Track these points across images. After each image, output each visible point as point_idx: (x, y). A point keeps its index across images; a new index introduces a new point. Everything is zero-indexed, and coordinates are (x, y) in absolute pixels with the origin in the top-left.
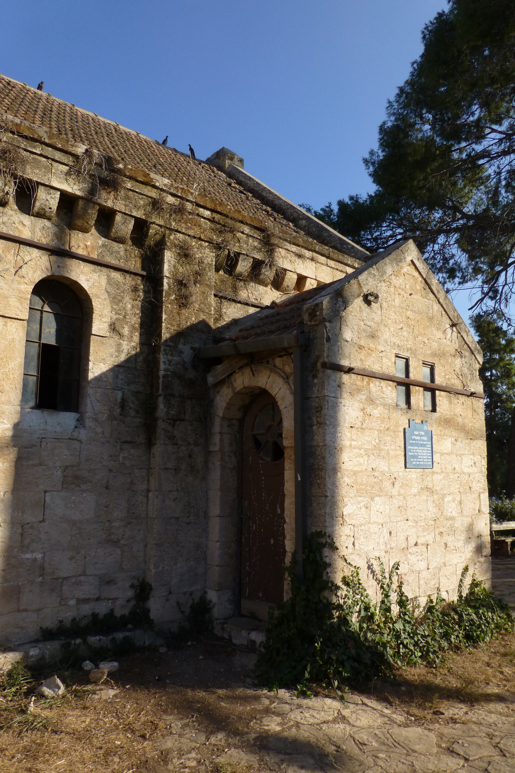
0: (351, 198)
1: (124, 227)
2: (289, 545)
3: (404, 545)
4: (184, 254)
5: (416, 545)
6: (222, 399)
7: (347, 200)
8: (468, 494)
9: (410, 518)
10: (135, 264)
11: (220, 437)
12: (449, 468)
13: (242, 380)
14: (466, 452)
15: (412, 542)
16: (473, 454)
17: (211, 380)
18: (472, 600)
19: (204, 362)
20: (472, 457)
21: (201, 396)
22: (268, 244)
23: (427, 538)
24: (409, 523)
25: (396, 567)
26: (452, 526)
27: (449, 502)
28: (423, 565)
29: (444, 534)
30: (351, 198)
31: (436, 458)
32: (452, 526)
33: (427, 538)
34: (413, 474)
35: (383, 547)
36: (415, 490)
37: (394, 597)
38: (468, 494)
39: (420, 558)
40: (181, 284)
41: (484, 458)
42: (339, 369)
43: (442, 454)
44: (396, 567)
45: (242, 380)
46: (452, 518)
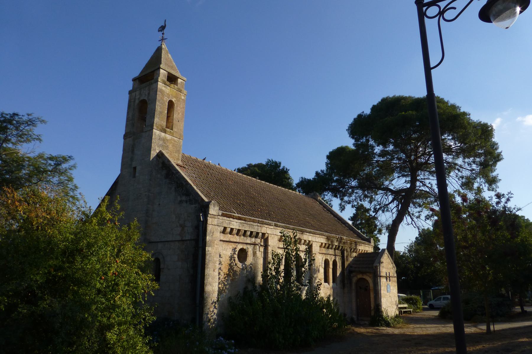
0: (321, 171)
1: (340, 248)
2: (372, 306)
4: (347, 251)
6: (354, 280)
7: (319, 171)
10: (340, 254)
11: (354, 287)
13: (360, 276)
17: (352, 275)
18: (396, 316)
19: (350, 272)
21: (350, 280)
22: (356, 245)
30: (321, 171)
34: (388, 294)
40: (347, 257)
42: (380, 276)
45: (360, 276)
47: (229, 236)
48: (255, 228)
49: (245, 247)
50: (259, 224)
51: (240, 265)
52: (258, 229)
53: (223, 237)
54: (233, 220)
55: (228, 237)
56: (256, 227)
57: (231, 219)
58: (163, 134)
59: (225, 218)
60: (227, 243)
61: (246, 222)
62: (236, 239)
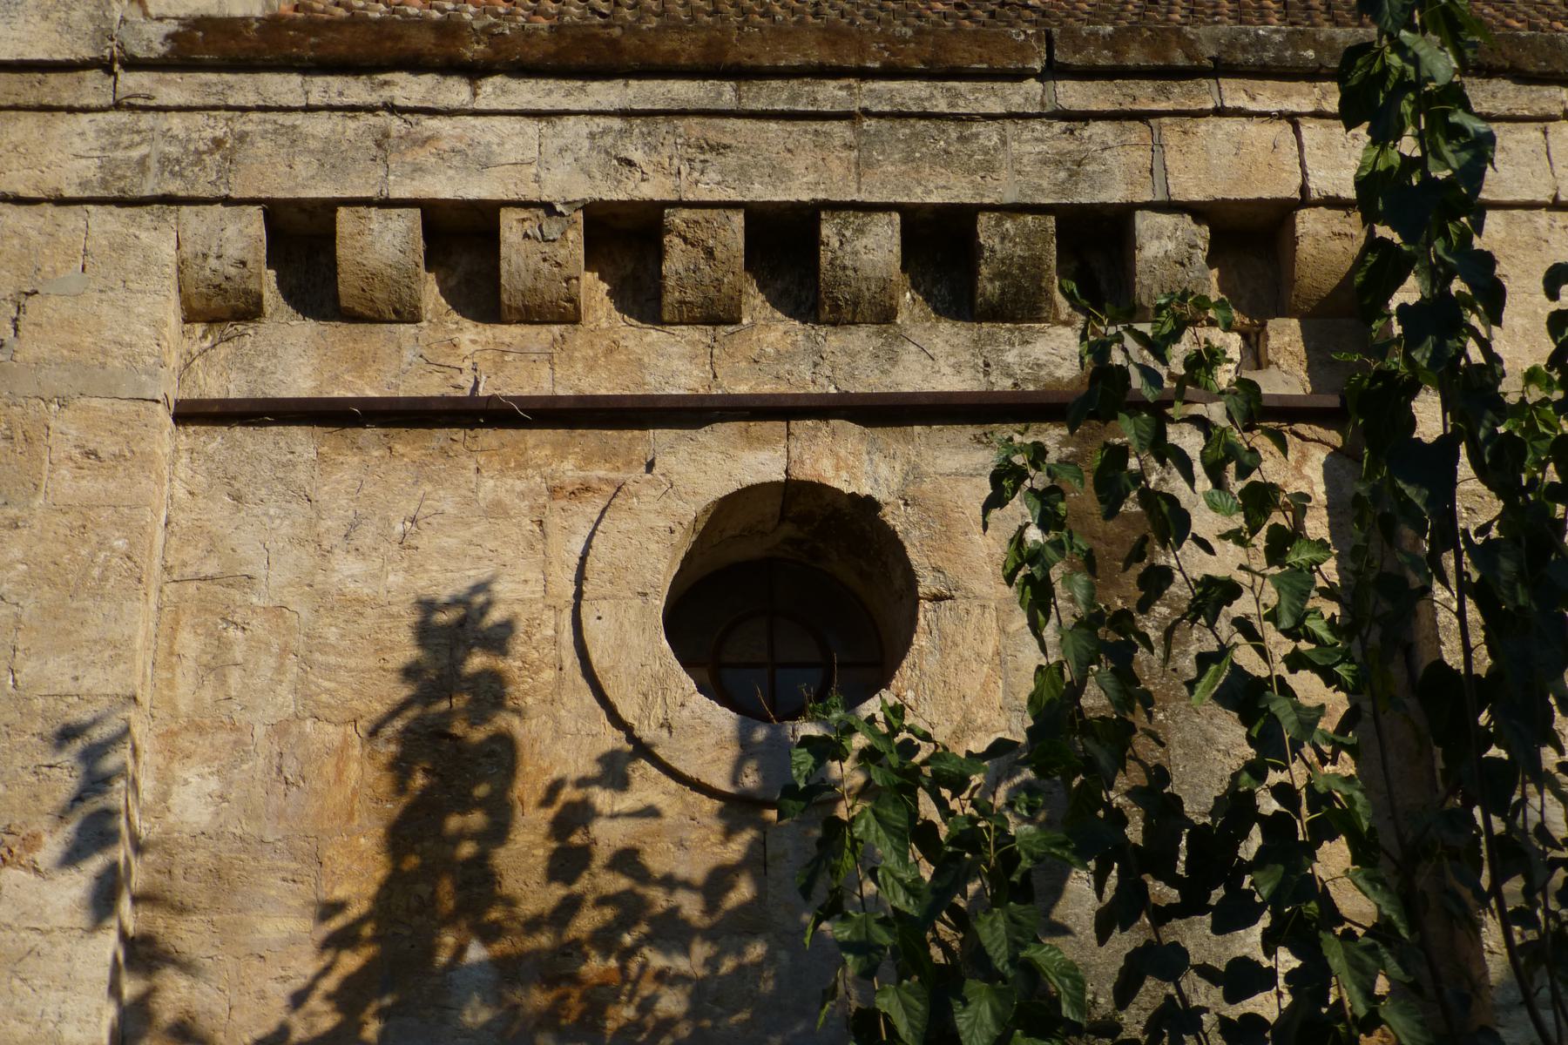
47: (471, 335)
48: (1011, 156)
49: (846, 463)
50: (1072, 94)
51: (704, 733)
52: (1076, 166)
53: (296, 357)
54: (456, 92)
55: (452, 352)
56: (1034, 142)
57: (409, 88)
59: (285, 87)
60: (410, 446)
61: (776, 95)
62: (624, 354)
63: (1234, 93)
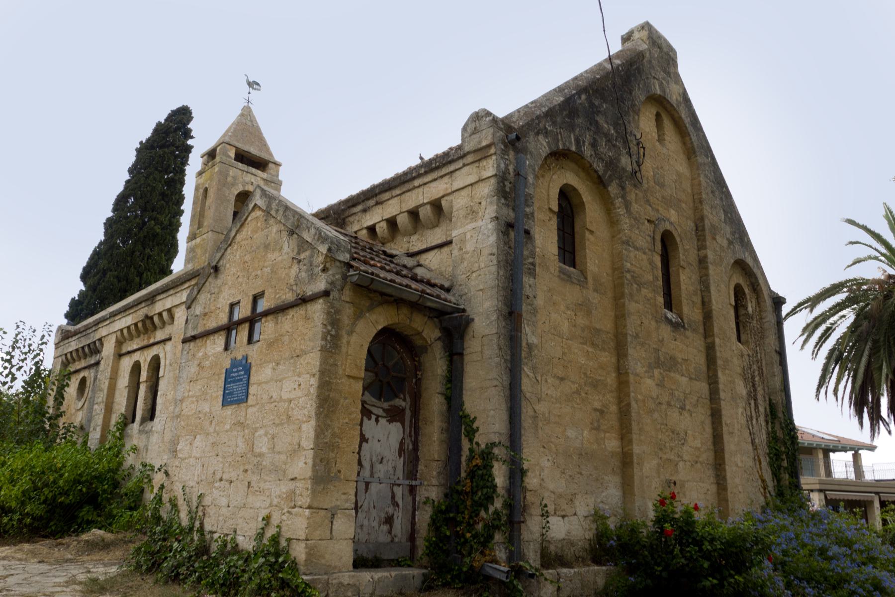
3: (212, 480)
5: (221, 480)
8: (286, 426)
9: (220, 454)
12: (265, 397)
14: (290, 374)
15: (218, 476)
16: (299, 375)
20: (296, 378)
23: (232, 475)
24: (219, 458)
25: (201, 497)
26: (259, 464)
27: (260, 436)
28: (224, 501)
29: (249, 472)
31: (252, 390)
32: (259, 464)
33: (232, 475)
35: (196, 479)
36: (228, 427)
37: (197, 524)
38: (286, 426)
39: (222, 493)
41: (314, 375)
43: (259, 384)
44: (201, 497)
46: (261, 455)
58: (194, 242)
63: (100, 325)
